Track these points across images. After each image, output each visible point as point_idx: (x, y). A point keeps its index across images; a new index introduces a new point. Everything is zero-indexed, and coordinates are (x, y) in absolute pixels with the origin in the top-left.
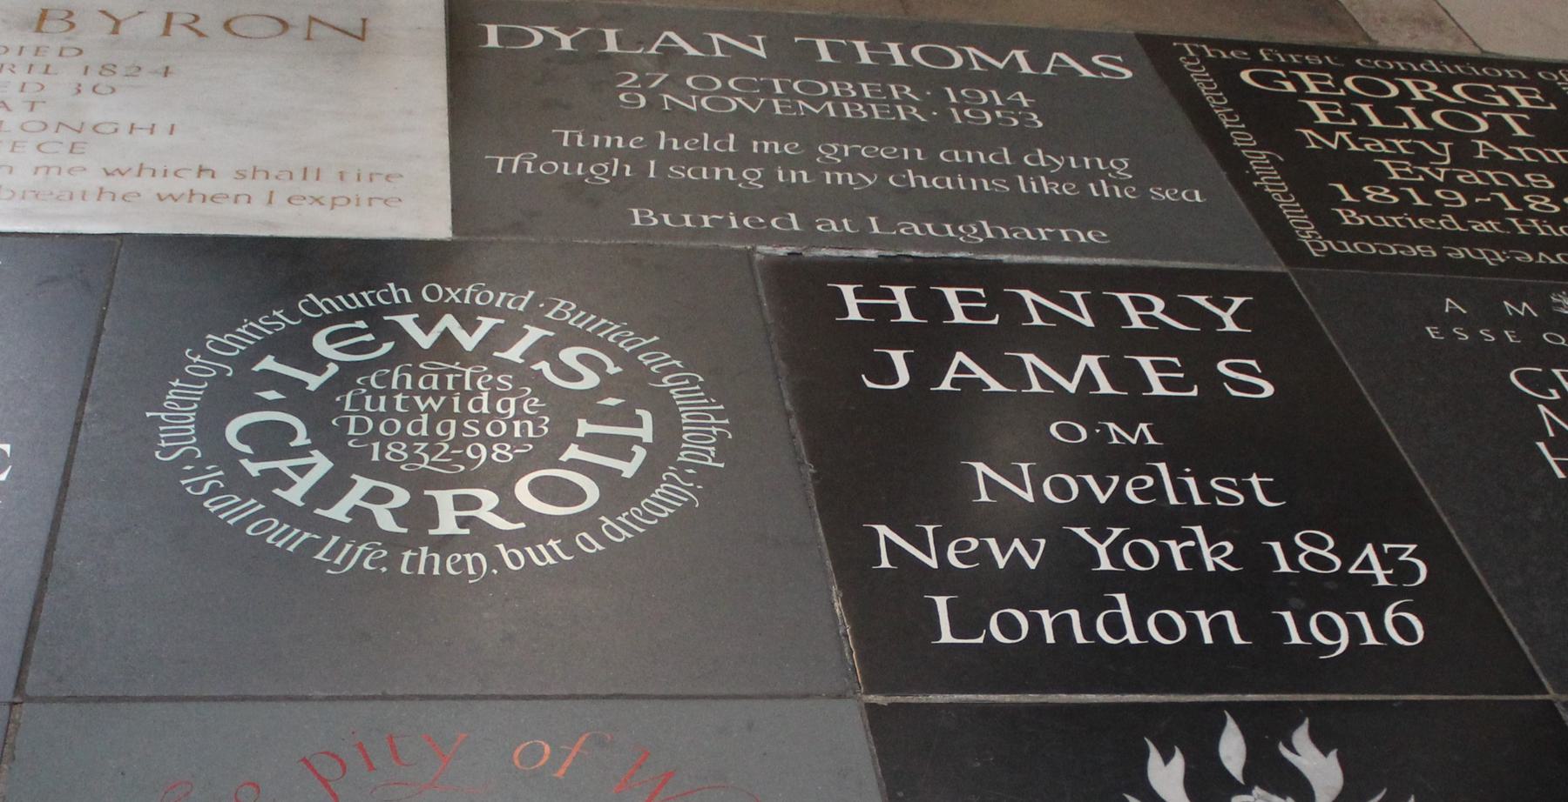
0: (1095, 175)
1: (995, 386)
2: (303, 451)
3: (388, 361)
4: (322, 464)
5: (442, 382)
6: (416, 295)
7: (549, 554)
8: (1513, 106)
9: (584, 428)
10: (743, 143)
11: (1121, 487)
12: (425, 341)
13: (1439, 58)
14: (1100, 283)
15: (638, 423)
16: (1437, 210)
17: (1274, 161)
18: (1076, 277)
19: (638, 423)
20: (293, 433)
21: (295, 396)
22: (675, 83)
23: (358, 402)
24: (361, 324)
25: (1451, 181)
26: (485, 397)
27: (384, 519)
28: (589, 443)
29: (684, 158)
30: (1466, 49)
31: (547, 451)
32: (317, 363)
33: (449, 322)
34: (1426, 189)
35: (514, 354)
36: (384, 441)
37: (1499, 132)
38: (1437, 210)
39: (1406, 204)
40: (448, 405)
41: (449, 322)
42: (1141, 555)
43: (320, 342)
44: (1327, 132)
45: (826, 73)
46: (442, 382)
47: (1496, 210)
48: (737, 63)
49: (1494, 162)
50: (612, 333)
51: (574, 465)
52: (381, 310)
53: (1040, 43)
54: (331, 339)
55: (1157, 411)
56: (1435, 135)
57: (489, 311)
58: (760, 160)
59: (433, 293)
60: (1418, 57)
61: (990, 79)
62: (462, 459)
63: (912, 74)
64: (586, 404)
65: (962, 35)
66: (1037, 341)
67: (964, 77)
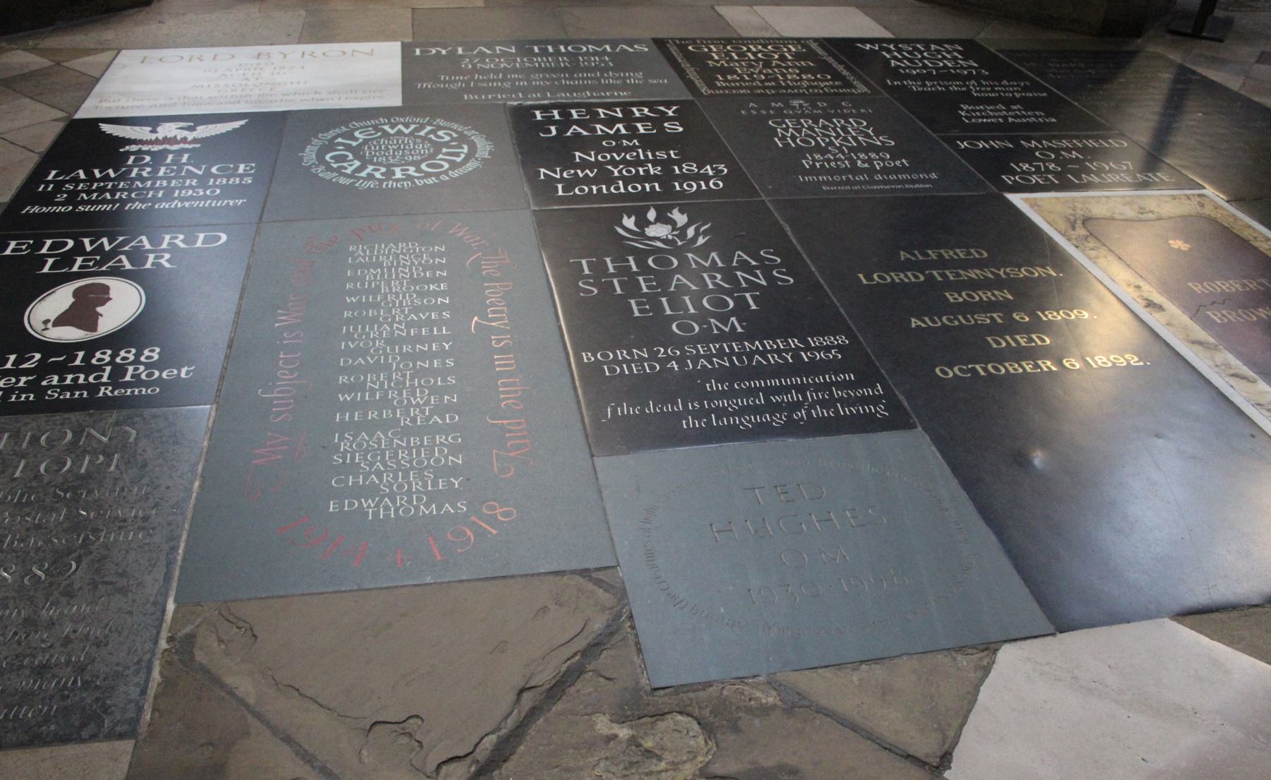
0: (630, 77)
1: (585, 133)
2: (352, 160)
3: (380, 137)
4: (357, 163)
5: (398, 141)
6: (389, 120)
7: (431, 181)
8: (789, 50)
9: (444, 150)
10: (505, 76)
11: (625, 156)
12: (392, 132)
13: (763, 39)
14: (626, 107)
15: (463, 148)
16: (754, 80)
17: (695, 70)
18: (618, 104)
19: (463, 148)
20: (347, 156)
21: (348, 148)
22: (483, 61)
23: (370, 148)
24: (371, 129)
25: (761, 72)
26: (412, 145)
27: (378, 175)
28: (447, 154)
29: (483, 81)
30: (776, 36)
31: (433, 156)
32: (356, 139)
33: (400, 127)
34: (751, 75)
35: (422, 133)
36: (378, 157)
37: (782, 58)
38: (754, 80)
39: (742, 79)
40: (399, 147)
41: (400, 127)
42: (629, 171)
43: (357, 134)
44: (718, 61)
45: (536, 55)
46: (398, 141)
47: (776, 79)
48: (504, 54)
49: (778, 66)
50: (455, 126)
51: (440, 159)
52: (377, 125)
53: (614, 44)
54: (360, 133)
55: (641, 138)
56: (757, 60)
57: (414, 123)
58: (511, 80)
59: (395, 120)
60: (755, 39)
61: (595, 53)
62: (404, 160)
63: (568, 54)
64: (447, 145)
65: (587, 42)
66: (602, 122)
67: (587, 53)
